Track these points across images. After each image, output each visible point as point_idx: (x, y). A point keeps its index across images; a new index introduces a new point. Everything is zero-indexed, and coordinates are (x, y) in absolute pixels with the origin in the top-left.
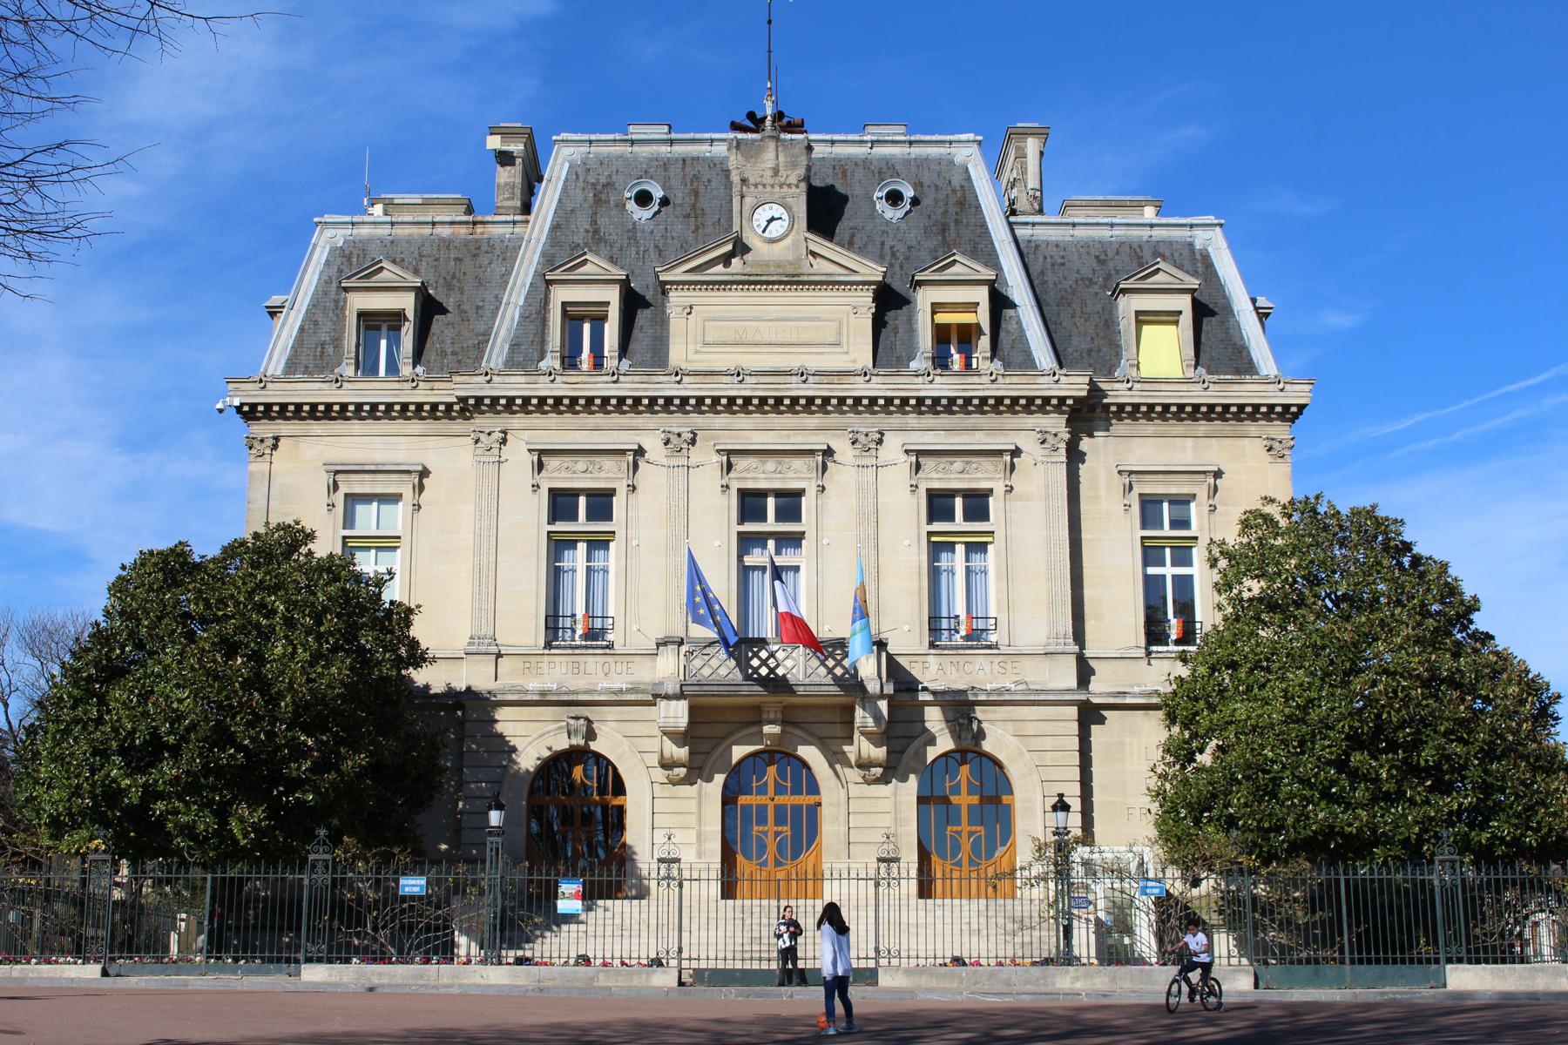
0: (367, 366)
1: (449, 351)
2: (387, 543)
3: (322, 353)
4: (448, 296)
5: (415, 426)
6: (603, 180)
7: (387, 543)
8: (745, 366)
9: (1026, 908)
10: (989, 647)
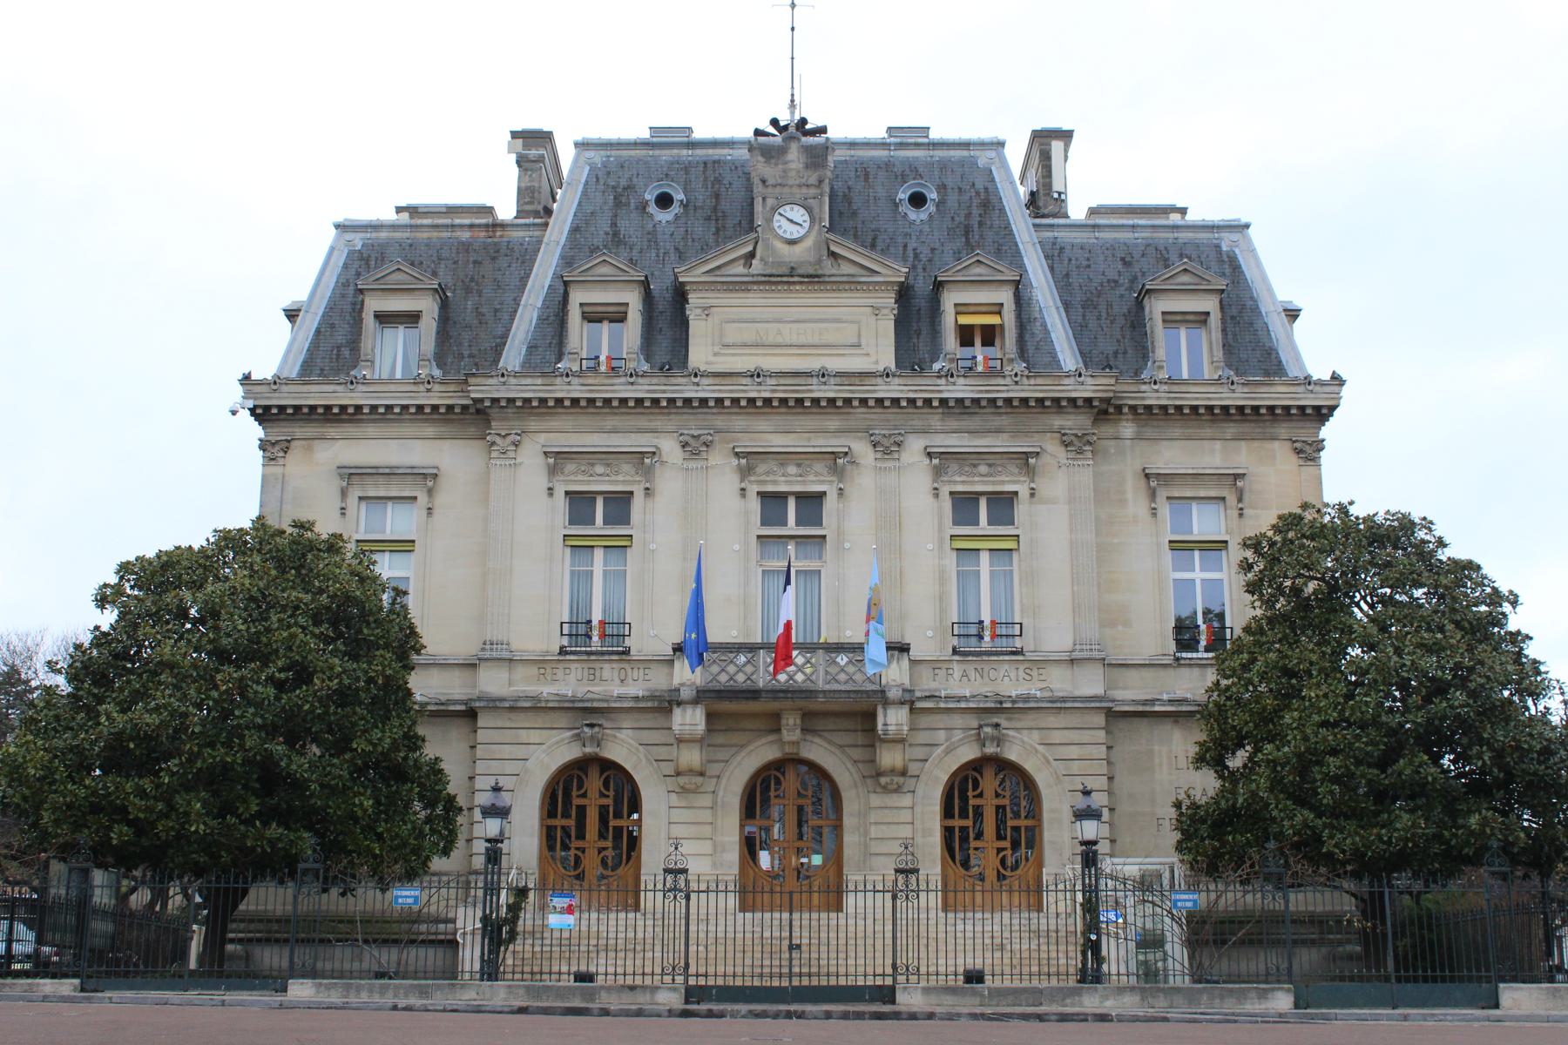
1: (466, 353)
2: (404, 546)
3: (338, 355)
4: (466, 299)
6: (623, 182)
7: (404, 546)
8: (765, 367)
9: (1052, 921)
10: (1013, 653)
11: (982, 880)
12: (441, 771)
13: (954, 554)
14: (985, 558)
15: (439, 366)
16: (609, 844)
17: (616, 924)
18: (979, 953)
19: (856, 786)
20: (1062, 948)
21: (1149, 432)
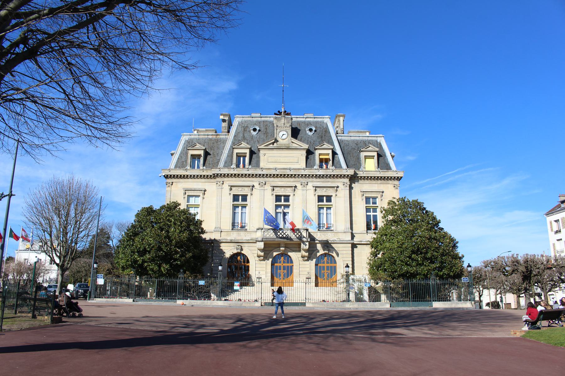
0: (192, 166)
2: (197, 206)
5: (203, 180)
7: (197, 206)
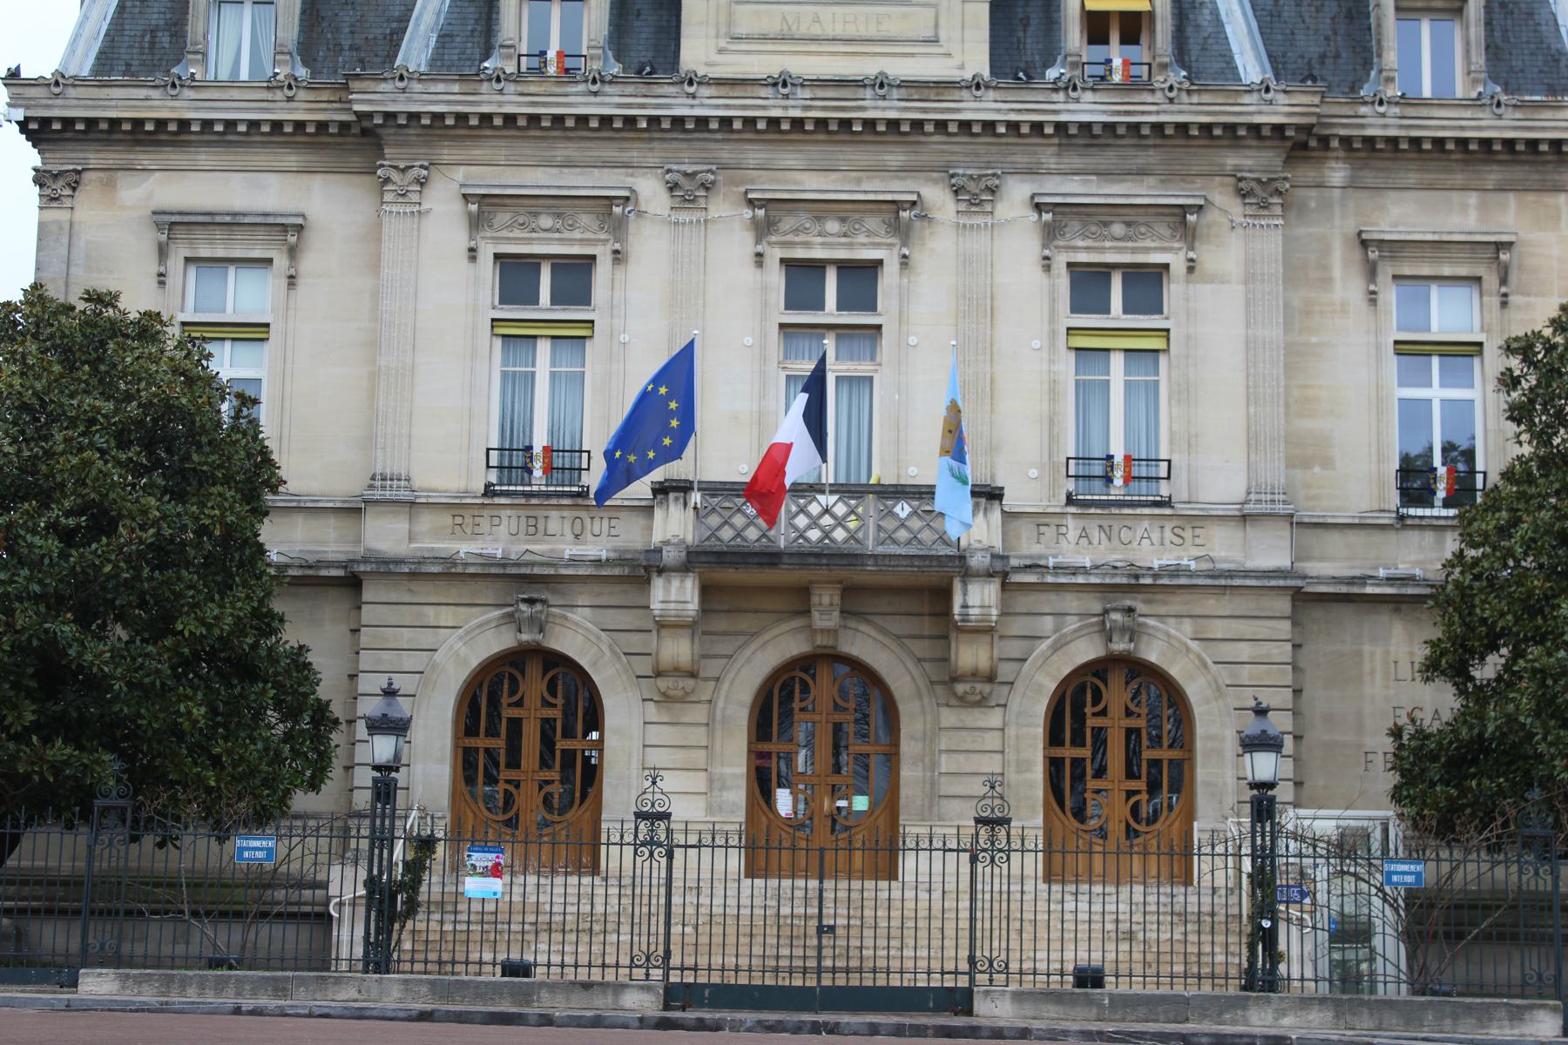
1: (346, 43)
2: (253, 332)
3: (153, 43)
7: (253, 332)
9: (1206, 900)
10: (1156, 504)
11: (1105, 837)
12: (307, 666)
13: (1072, 354)
14: (1117, 361)
15: (305, 63)
16: (555, 775)
17: (562, 893)
18: (1096, 944)
19: (920, 696)
20: (1220, 939)
21: (1369, 177)
